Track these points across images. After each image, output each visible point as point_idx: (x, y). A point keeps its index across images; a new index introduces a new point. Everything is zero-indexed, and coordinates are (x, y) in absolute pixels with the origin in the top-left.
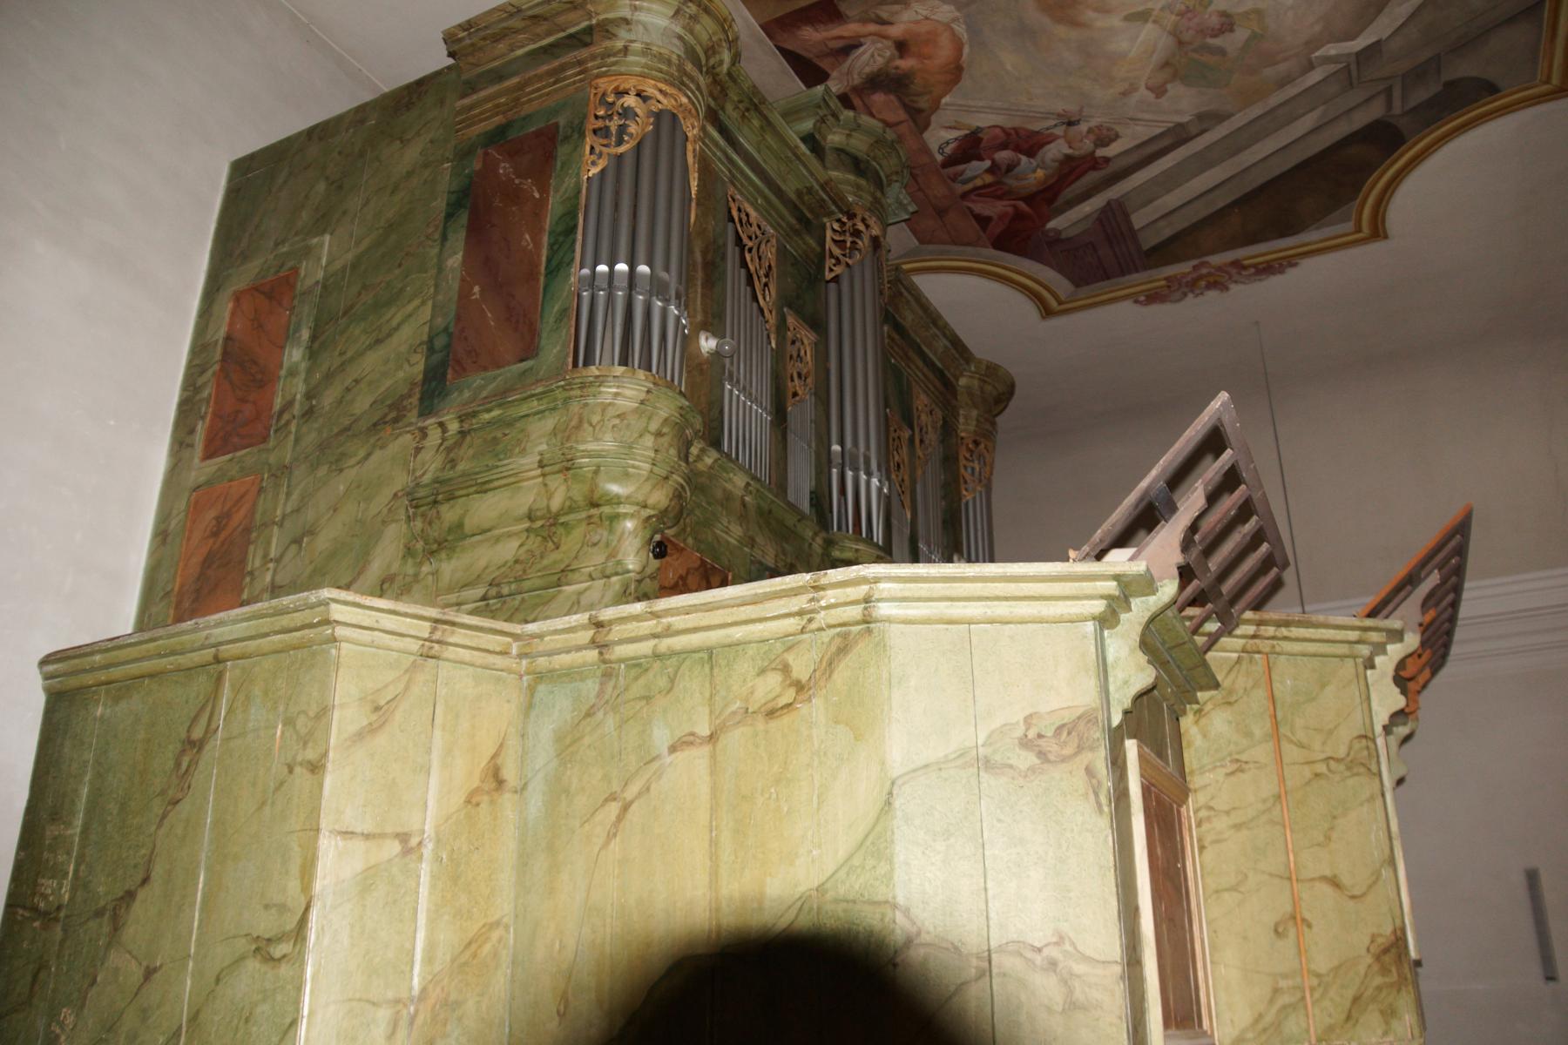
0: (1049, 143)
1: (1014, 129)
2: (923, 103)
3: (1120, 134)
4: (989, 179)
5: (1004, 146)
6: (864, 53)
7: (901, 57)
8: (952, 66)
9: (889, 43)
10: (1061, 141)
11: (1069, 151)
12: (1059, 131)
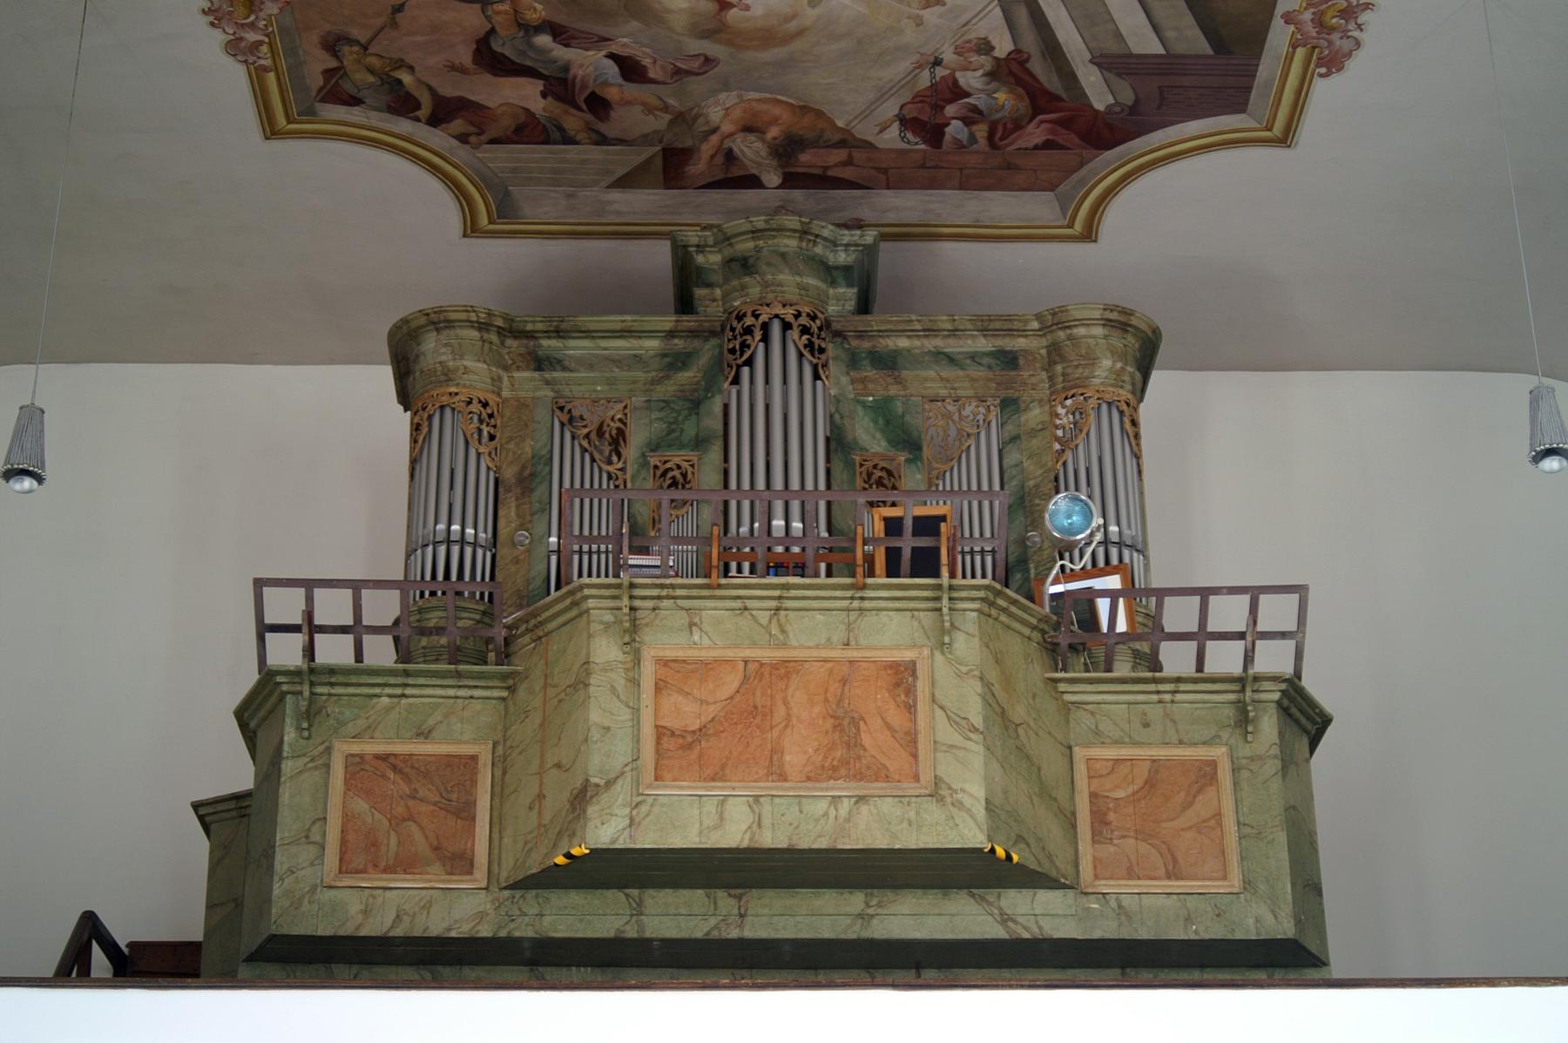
0: (955, 82)
1: (914, 98)
2: (837, 137)
3: (983, 36)
4: (981, 130)
5: (938, 108)
6: (741, 151)
7: (764, 133)
8: (797, 110)
9: (741, 135)
10: (958, 75)
11: (980, 72)
12: (941, 72)
